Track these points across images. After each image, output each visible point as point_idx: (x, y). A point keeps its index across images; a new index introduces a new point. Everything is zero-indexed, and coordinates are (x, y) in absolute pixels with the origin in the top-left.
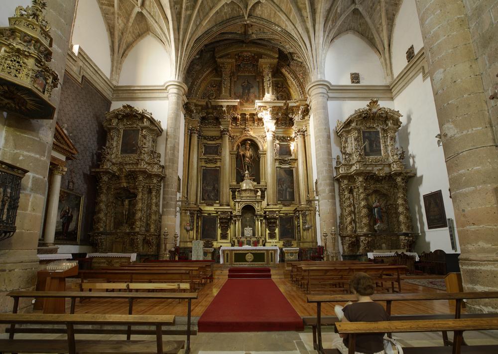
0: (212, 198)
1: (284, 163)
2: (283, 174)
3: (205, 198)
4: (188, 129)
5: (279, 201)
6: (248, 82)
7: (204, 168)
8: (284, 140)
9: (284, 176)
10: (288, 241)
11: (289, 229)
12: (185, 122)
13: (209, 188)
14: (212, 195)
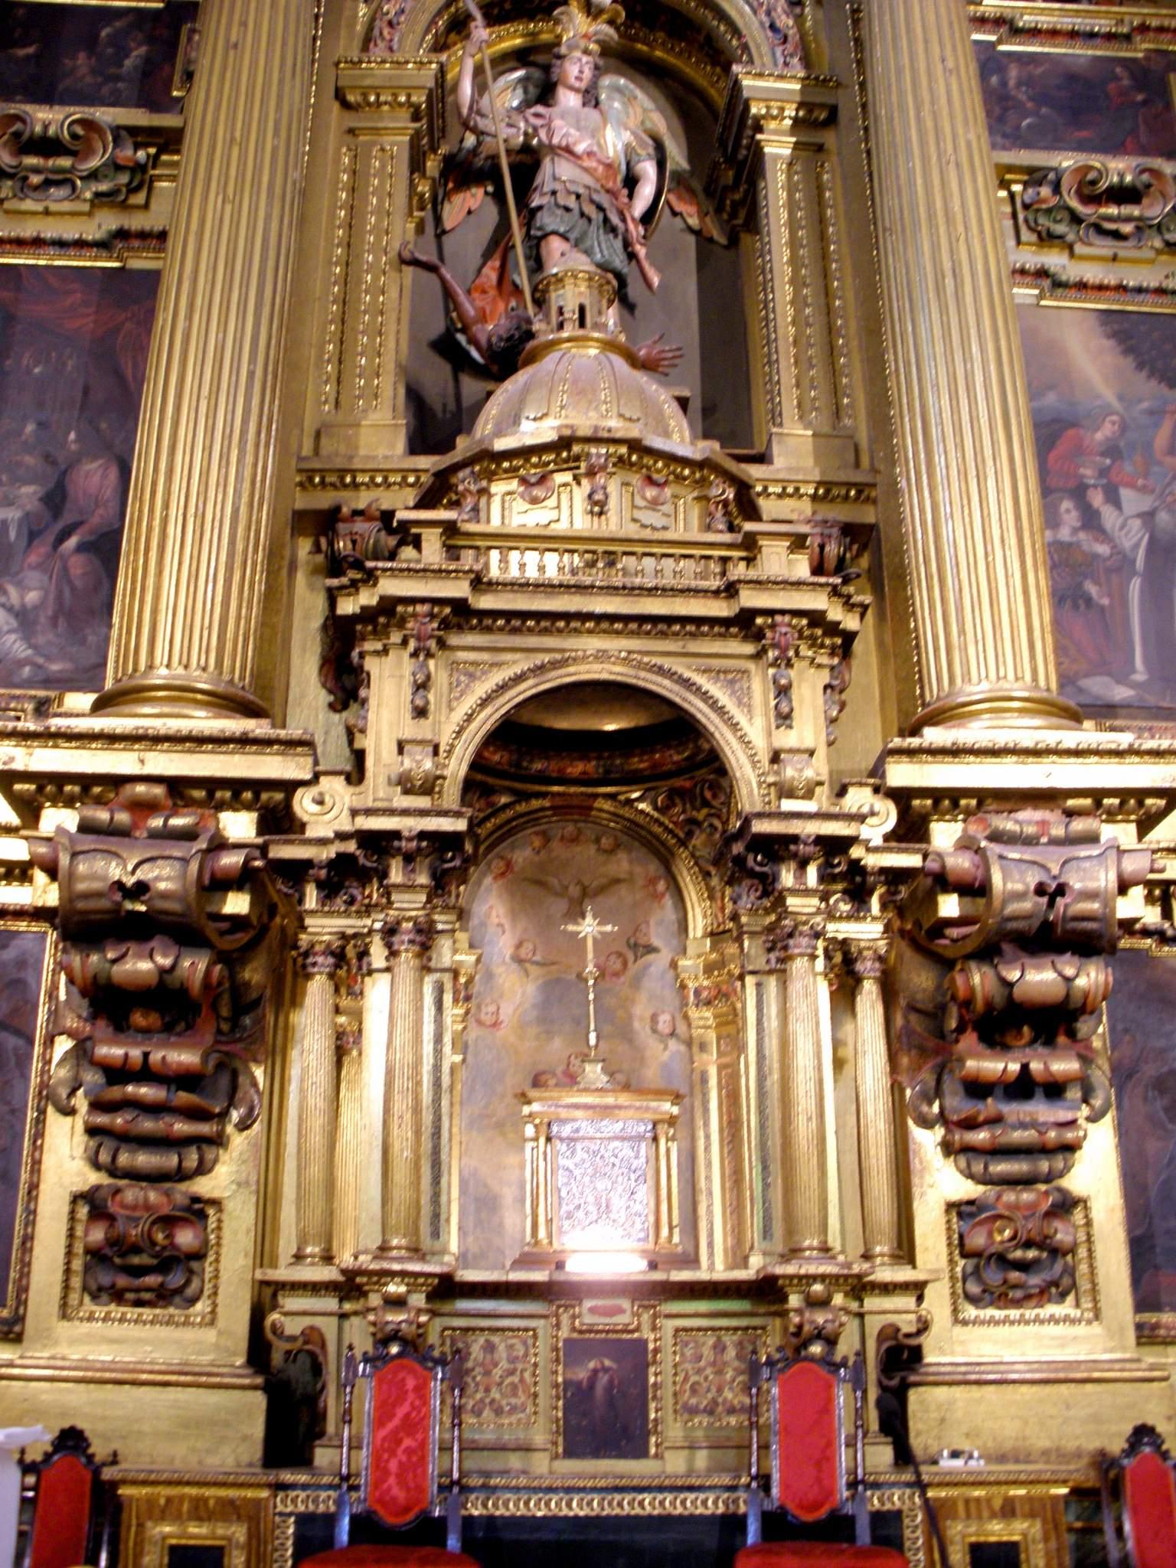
9: (1109, 395)
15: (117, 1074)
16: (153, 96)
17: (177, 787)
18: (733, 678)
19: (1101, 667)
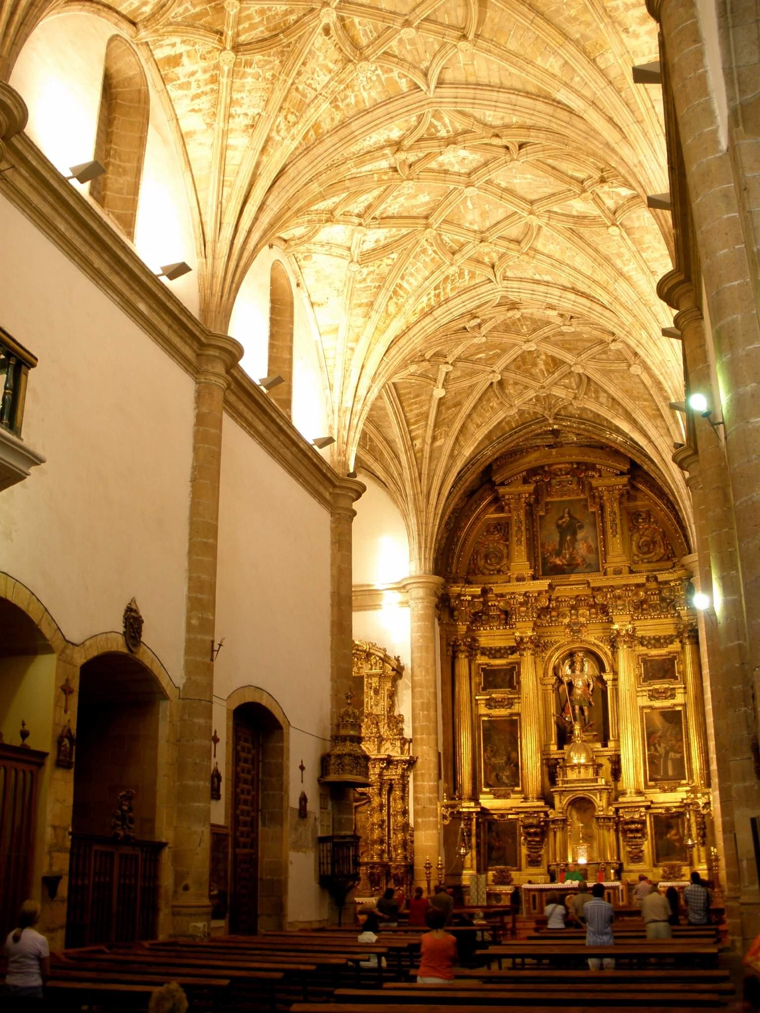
0: (506, 781)
1: (657, 699)
2: (658, 721)
3: (490, 783)
4: (448, 645)
5: (650, 780)
6: (570, 516)
7: (486, 719)
8: (657, 645)
10: (672, 867)
11: (674, 840)
12: (441, 630)
13: (500, 761)
14: (505, 776)
15: (530, 841)
16: (511, 686)
17: (535, 812)
18: (595, 795)
19: (656, 773)
